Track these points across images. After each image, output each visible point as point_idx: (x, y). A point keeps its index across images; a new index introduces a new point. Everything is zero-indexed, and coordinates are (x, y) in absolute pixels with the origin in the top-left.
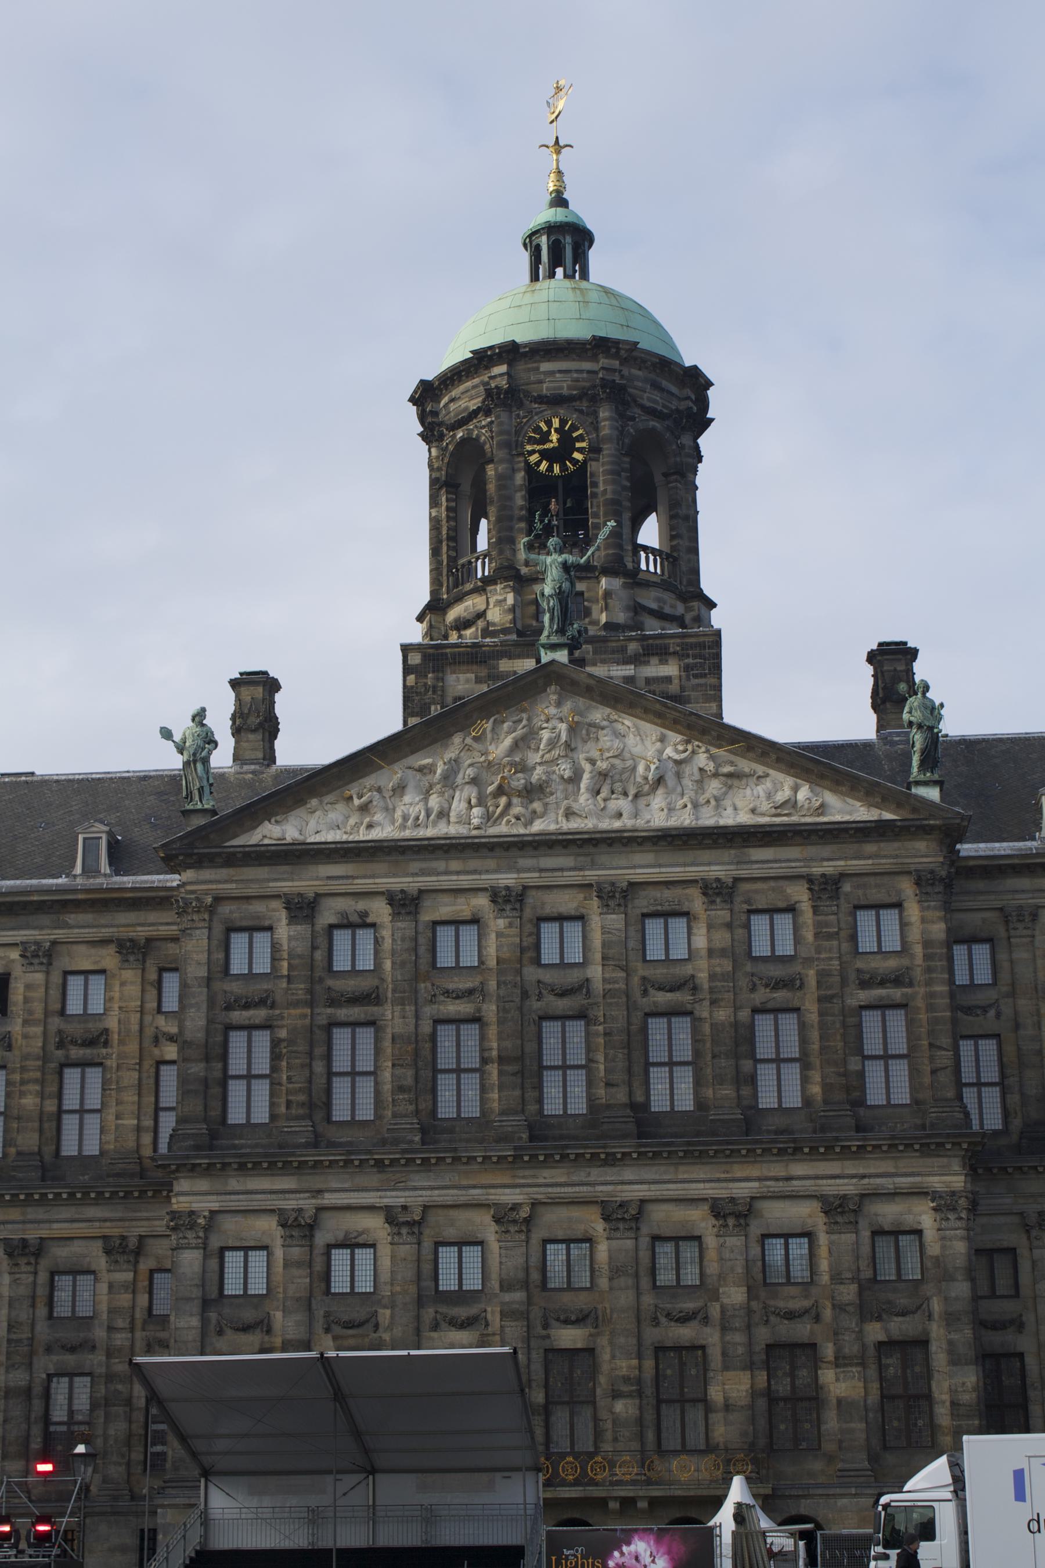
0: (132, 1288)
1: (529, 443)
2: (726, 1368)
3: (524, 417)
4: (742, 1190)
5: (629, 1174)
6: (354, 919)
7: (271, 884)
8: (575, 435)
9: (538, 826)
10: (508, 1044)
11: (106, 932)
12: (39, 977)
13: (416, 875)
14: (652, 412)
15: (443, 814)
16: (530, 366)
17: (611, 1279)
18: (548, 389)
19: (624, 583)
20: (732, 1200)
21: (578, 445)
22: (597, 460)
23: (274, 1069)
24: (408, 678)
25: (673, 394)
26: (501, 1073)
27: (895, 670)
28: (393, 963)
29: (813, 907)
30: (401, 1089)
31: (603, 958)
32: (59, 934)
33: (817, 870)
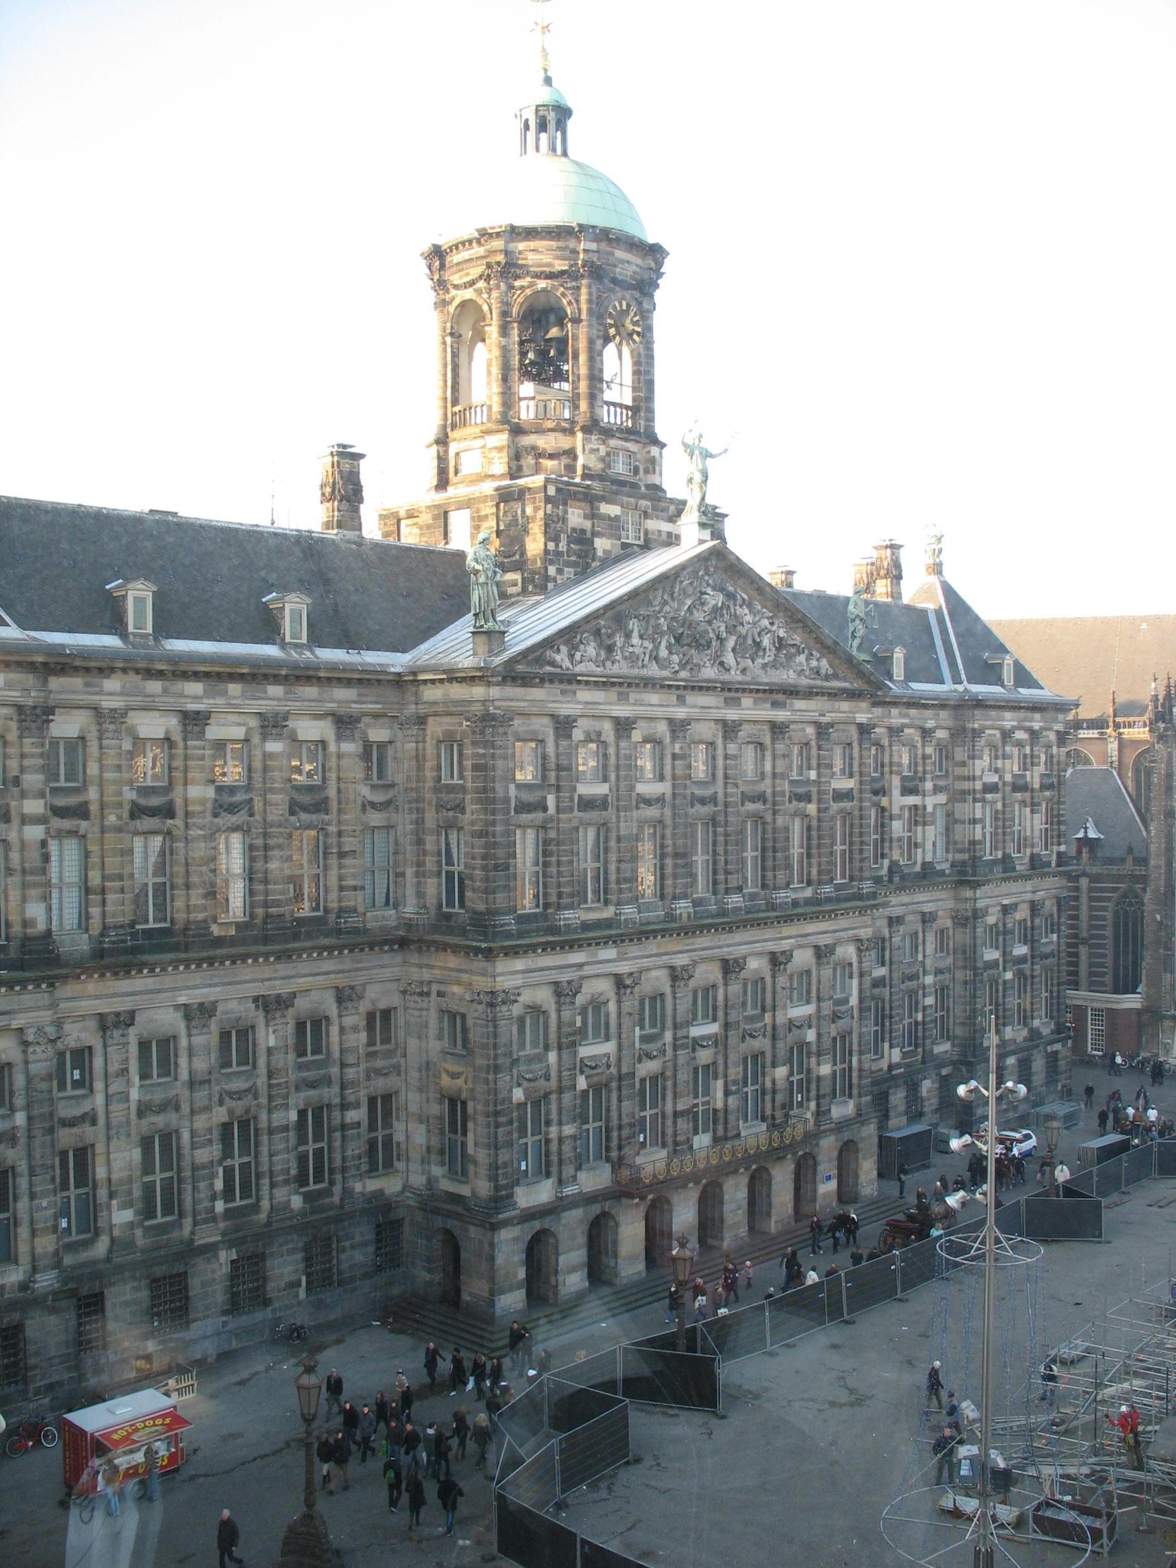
0: (355, 1029)
2: (774, 1065)
4: (786, 945)
5: (738, 937)
10: (680, 842)
11: (332, 706)
12: (274, 746)
17: (726, 1014)
20: (783, 953)
23: (546, 864)
26: (675, 866)
28: (618, 777)
30: (626, 880)
31: (726, 777)
32: (292, 706)
33: (823, 720)
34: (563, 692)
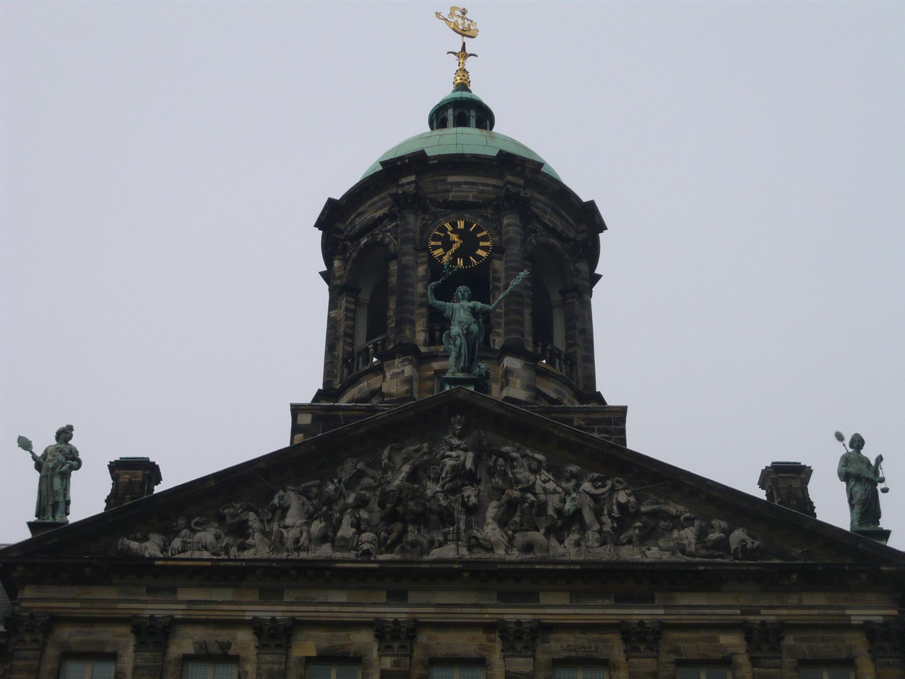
1: (433, 240)
3: (429, 220)
6: (214, 649)
7: (121, 606)
8: (479, 235)
9: (436, 553)
13: (292, 603)
14: (551, 231)
15: (324, 538)
16: (437, 178)
18: (453, 197)
19: (525, 364)
21: (482, 244)
22: (500, 259)
24: (296, 437)
25: (571, 225)
27: (791, 486)
29: (752, 659)
34: (151, 590)
